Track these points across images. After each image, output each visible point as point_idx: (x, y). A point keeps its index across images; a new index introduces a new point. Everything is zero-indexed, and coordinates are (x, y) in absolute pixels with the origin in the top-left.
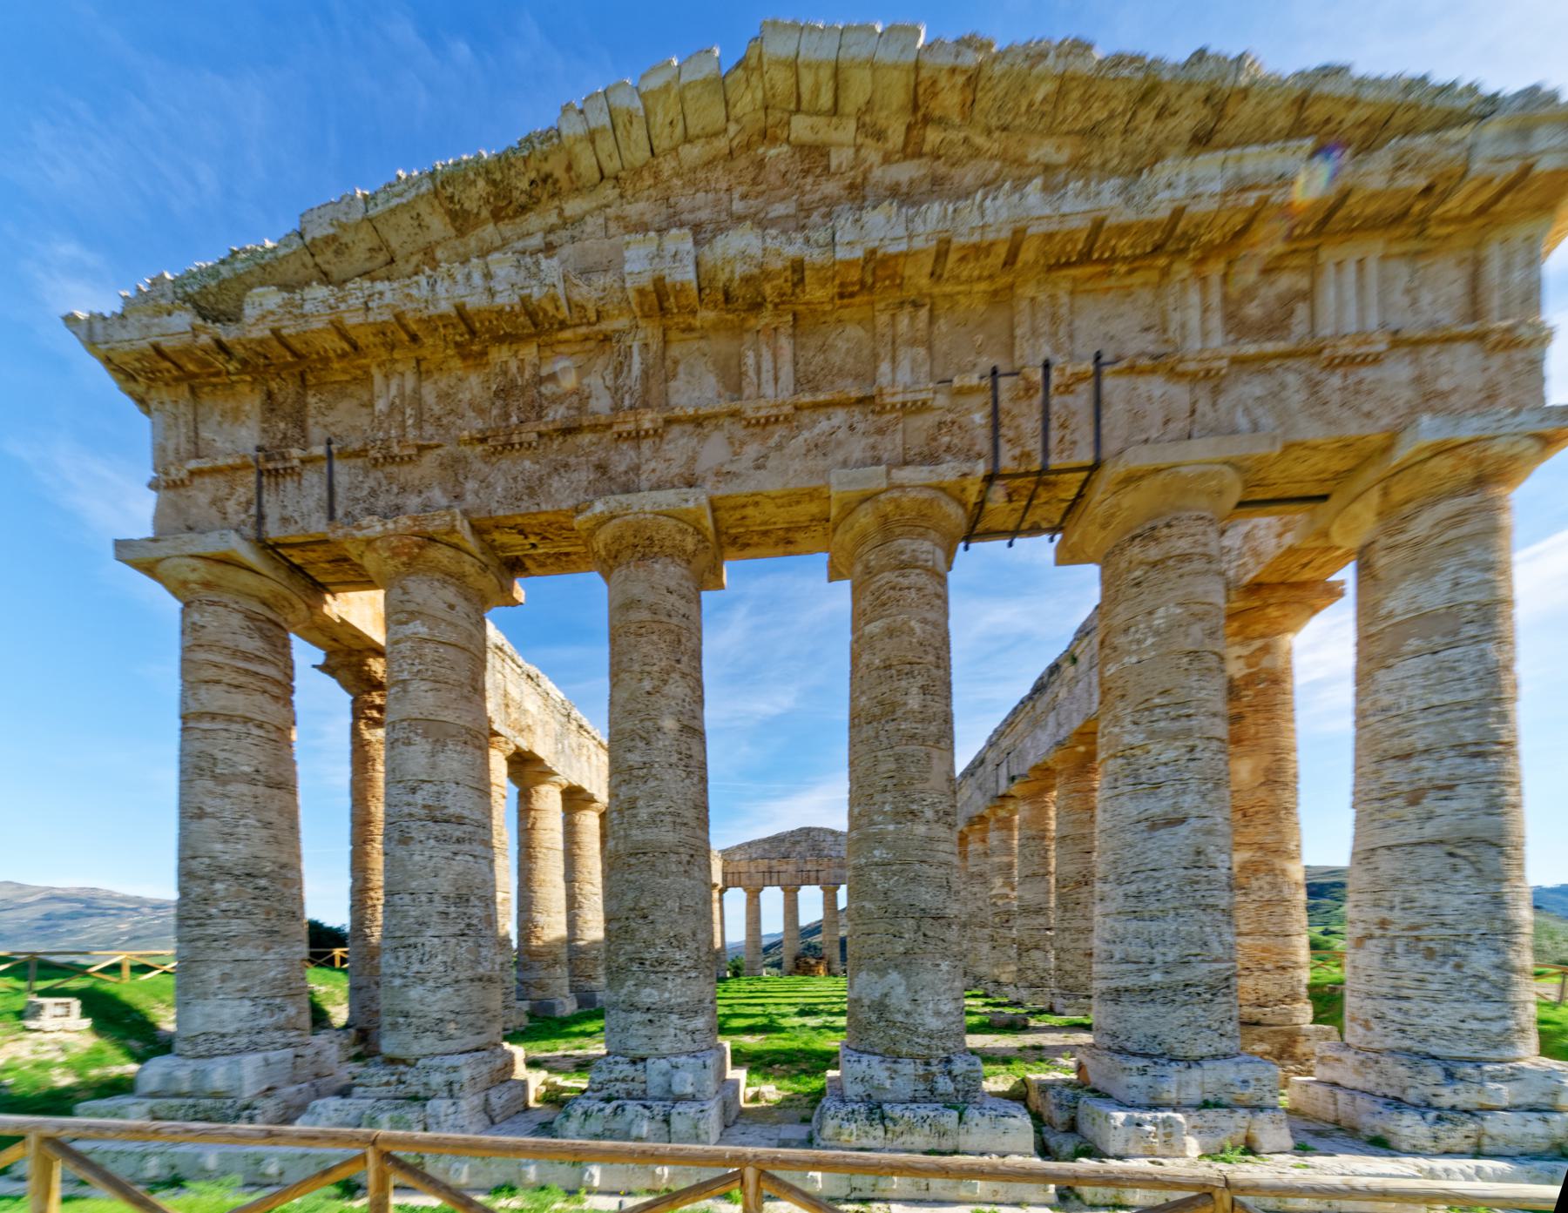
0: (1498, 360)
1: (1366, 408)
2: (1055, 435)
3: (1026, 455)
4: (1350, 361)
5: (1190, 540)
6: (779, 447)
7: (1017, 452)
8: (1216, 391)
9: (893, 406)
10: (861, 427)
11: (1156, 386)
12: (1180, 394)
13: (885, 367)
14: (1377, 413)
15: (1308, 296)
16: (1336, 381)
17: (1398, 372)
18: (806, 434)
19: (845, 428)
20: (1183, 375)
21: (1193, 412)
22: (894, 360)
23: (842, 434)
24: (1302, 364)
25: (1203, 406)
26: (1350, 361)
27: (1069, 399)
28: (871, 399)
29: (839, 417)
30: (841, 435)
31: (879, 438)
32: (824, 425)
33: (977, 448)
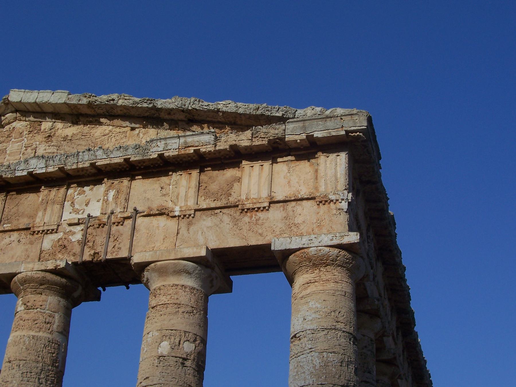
0: (324, 208)
1: (260, 231)
2: (111, 245)
5: (169, 297)
7: (92, 252)
8: (190, 224)
9: (39, 232)
10: (23, 241)
11: (162, 221)
12: (172, 224)
13: (40, 214)
14: (265, 234)
15: (239, 180)
16: (246, 219)
17: (276, 214)
19: (16, 241)
20: (175, 217)
22: (45, 210)
24: (232, 211)
25: (183, 231)
27: (120, 227)
28: (29, 229)
29: (15, 235)
30: (13, 244)
31: (30, 246)
32: (7, 240)
33: (74, 251)
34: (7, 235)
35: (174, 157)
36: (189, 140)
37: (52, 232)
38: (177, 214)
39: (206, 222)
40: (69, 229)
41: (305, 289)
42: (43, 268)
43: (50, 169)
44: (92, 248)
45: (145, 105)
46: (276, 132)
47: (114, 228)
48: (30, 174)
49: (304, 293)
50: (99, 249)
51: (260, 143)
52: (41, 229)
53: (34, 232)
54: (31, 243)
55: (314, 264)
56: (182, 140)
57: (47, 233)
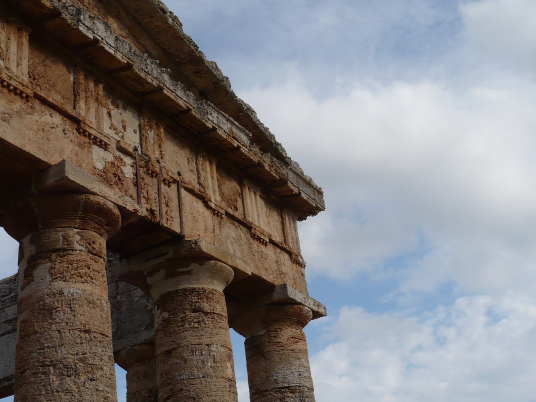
0: (295, 266)
3: (151, 211)
4: (259, 239)
6: (19, 114)
7: (148, 206)
15: (241, 195)
18: (36, 117)
21: (214, 230)
23: (58, 132)
26: (259, 239)
29: (57, 119)
34: (47, 111)
35: (223, 139)
36: (234, 130)
37: (105, 146)
38: (213, 206)
39: (231, 231)
40: (118, 154)
41: (294, 343)
42: (121, 204)
43: (119, 56)
44: (148, 199)
45: (193, 48)
46: (284, 172)
47: (163, 186)
48: (96, 41)
49: (294, 347)
50: (155, 207)
51: (274, 175)
52: (93, 132)
53: (85, 131)
54: (80, 145)
55: (298, 321)
56: (229, 125)
57: (95, 143)
